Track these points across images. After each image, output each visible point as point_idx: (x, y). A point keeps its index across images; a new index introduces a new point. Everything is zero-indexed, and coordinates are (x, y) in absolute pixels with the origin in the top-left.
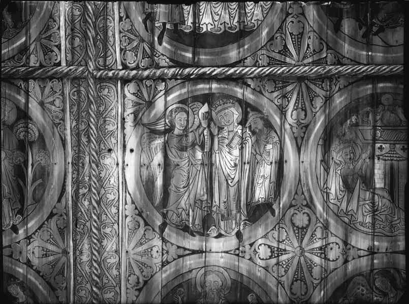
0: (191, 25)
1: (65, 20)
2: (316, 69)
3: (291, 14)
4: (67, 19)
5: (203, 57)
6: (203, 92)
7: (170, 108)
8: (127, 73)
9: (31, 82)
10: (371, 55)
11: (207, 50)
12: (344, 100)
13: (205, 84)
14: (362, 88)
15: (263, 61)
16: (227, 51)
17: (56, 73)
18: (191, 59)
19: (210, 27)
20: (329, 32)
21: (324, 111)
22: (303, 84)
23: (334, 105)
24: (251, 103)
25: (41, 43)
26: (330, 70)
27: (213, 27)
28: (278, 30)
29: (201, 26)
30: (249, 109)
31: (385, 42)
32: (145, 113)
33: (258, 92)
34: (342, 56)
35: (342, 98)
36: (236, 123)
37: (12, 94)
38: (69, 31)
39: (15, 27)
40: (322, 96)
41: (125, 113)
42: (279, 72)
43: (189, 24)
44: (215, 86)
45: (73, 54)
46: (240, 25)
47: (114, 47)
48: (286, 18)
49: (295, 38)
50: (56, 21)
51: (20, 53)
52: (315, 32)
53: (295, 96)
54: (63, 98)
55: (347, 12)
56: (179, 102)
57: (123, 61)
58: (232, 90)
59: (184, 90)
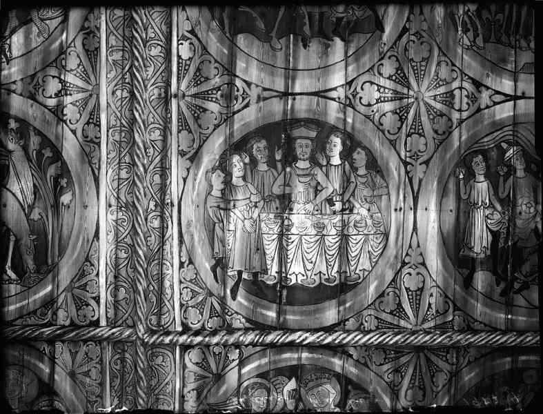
0: (276, 275)
1: (107, 264)
2: (440, 340)
3: (409, 263)
4: (109, 262)
5: (290, 317)
6: (289, 364)
7: (245, 384)
8: (189, 340)
9: (59, 345)
10: (511, 319)
11: (296, 308)
12: (474, 375)
13: (292, 353)
14: (498, 362)
15: (370, 323)
16: (322, 311)
17: (94, 336)
18: (275, 320)
19: (300, 278)
20: (458, 288)
21: (449, 391)
22: (421, 354)
23: (461, 383)
24: (354, 379)
25: (73, 294)
26: (459, 341)
27: (303, 278)
28: (390, 284)
29: (288, 276)
30: (350, 387)
31: (528, 302)
32: (212, 390)
33: (362, 364)
34: (474, 319)
35: (473, 374)
36: (332, 406)
37: (33, 361)
38: (111, 279)
39: (38, 271)
40: (446, 371)
41: (185, 389)
42: (391, 342)
43: (274, 273)
44: (305, 355)
45: (116, 308)
46: (340, 276)
47: (171, 302)
48: (401, 268)
49: (412, 295)
50: (93, 266)
51: (44, 306)
52: (439, 287)
53: (411, 371)
54: (102, 368)
55: (481, 263)
56: (258, 376)
57: (184, 320)
58: (329, 362)
59: (265, 361)
